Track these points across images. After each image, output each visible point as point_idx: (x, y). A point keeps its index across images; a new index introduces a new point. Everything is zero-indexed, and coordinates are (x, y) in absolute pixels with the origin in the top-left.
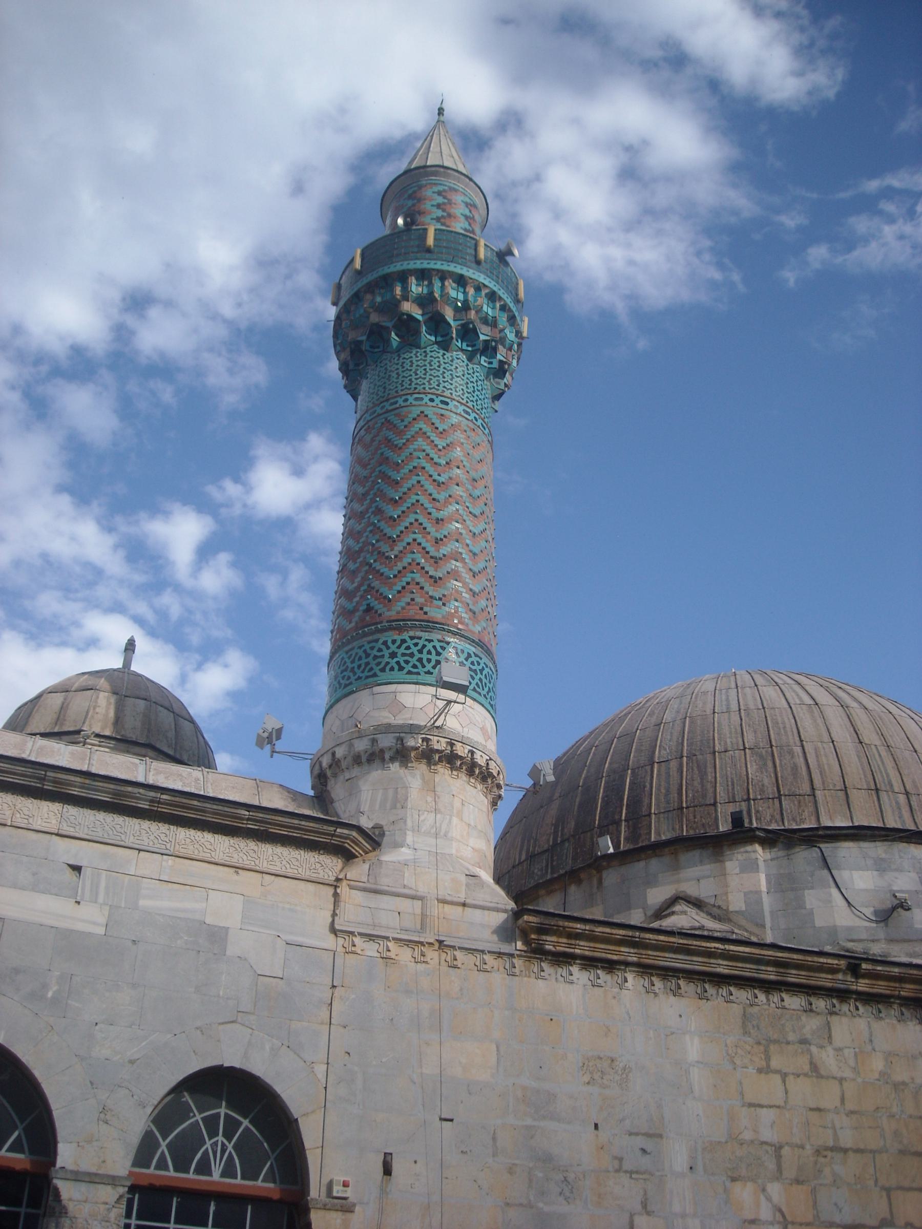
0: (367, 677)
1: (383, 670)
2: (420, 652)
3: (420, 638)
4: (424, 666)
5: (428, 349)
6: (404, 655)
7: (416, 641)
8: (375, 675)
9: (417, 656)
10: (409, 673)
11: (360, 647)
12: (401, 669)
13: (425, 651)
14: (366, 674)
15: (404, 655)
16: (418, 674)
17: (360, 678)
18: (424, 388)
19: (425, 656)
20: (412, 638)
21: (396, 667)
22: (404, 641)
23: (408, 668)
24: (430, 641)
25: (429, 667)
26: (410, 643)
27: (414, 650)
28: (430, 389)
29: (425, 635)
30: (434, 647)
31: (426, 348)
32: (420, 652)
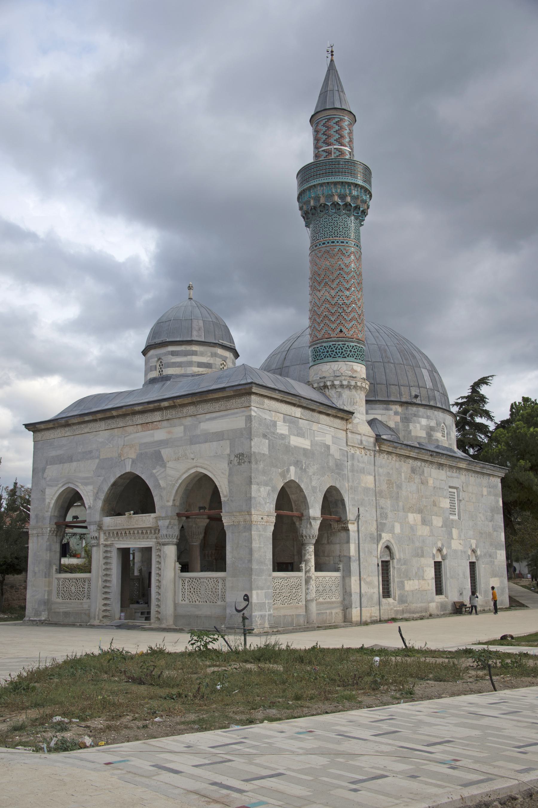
0: (320, 359)
1: (325, 357)
2: (336, 349)
3: (336, 344)
4: (338, 355)
5: (333, 217)
6: (331, 351)
7: (334, 345)
8: (323, 359)
9: (335, 351)
10: (333, 357)
11: (318, 348)
12: (331, 356)
13: (338, 349)
14: (320, 358)
15: (331, 351)
16: (336, 357)
17: (318, 359)
18: (332, 237)
19: (338, 351)
20: (333, 345)
21: (329, 356)
22: (330, 346)
23: (333, 356)
24: (339, 345)
25: (339, 355)
26: (332, 347)
27: (334, 349)
28: (335, 237)
29: (337, 343)
30: (341, 347)
31: (332, 216)
32: (336, 349)
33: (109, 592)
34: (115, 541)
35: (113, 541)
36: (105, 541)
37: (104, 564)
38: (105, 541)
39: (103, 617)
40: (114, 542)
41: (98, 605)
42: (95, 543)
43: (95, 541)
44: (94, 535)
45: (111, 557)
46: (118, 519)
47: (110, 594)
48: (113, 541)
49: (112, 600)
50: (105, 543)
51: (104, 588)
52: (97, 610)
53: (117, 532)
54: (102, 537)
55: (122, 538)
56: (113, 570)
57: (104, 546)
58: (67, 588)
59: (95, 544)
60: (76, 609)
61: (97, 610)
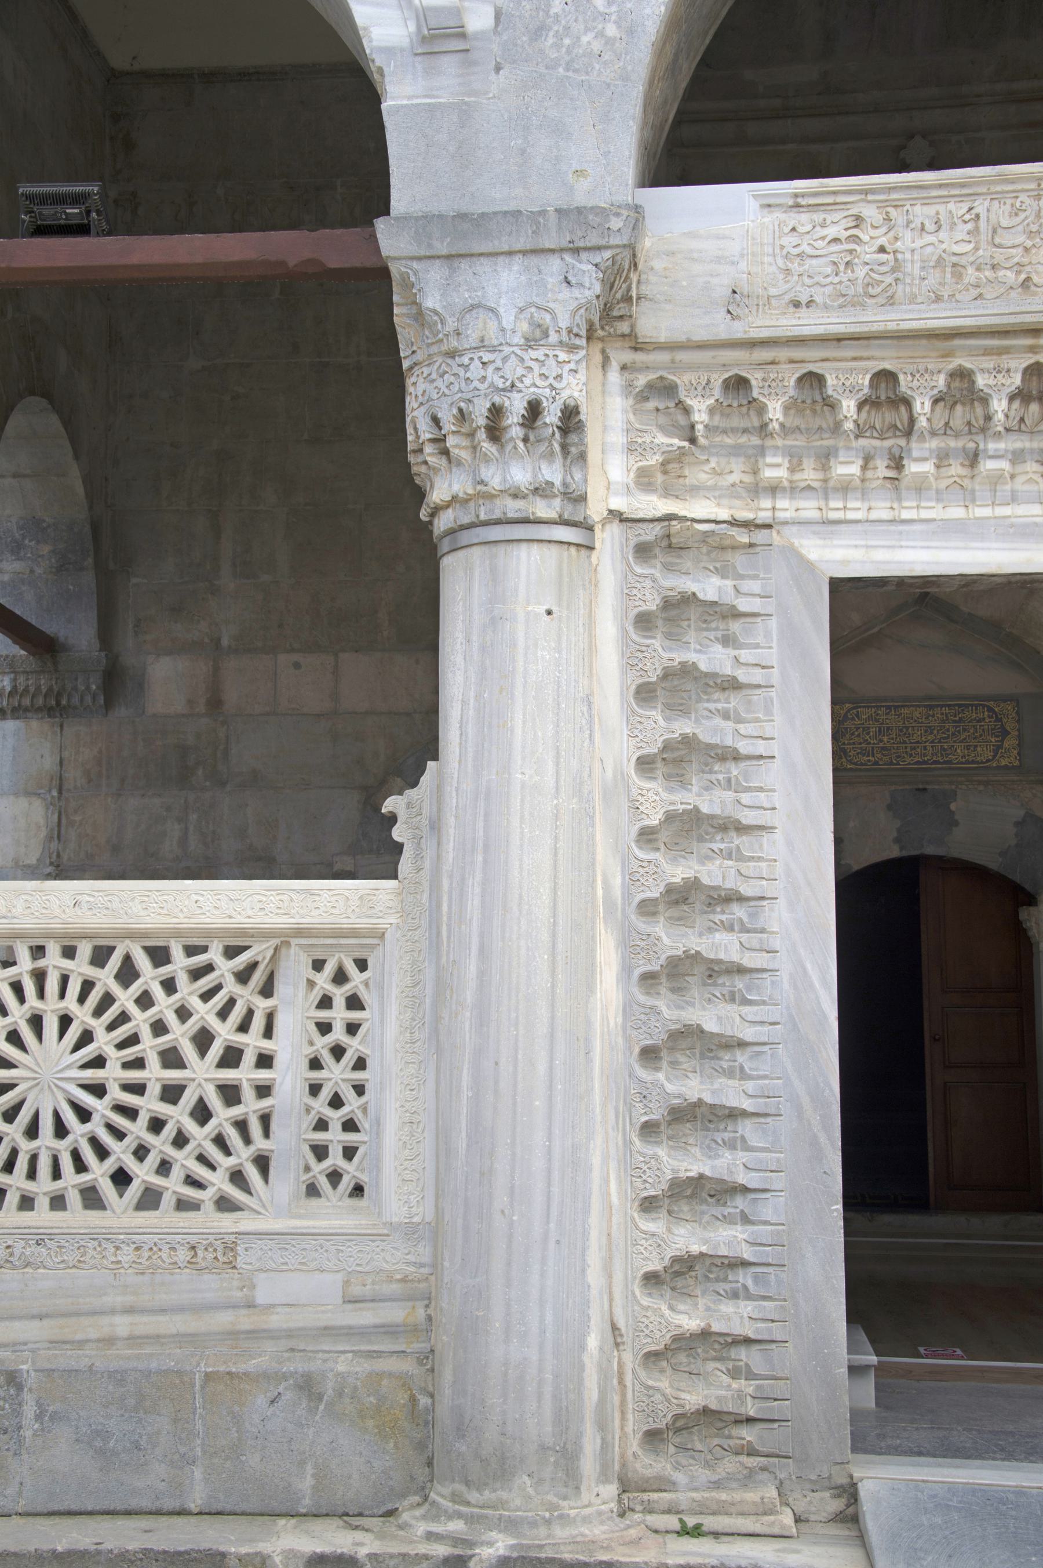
33: (734, 1114)
34: (794, 490)
35: (774, 489)
36: (644, 480)
37: (645, 764)
38: (644, 480)
39: (653, 1437)
40: (786, 507)
41: (594, 1277)
42: (542, 490)
43: (553, 473)
44: (534, 386)
45: (732, 685)
46: (922, 213)
47: (746, 1128)
48: (774, 489)
49: (769, 1209)
50: (658, 505)
51: (649, 1055)
52: (593, 1342)
53: (885, 377)
54: (617, 438)
55: (942, 459)
56: (773, 846)
57: (643, 551)
58: (231, 1057)
59: (542, 509)
60: (122, 1325)
61: (593, 1342)
